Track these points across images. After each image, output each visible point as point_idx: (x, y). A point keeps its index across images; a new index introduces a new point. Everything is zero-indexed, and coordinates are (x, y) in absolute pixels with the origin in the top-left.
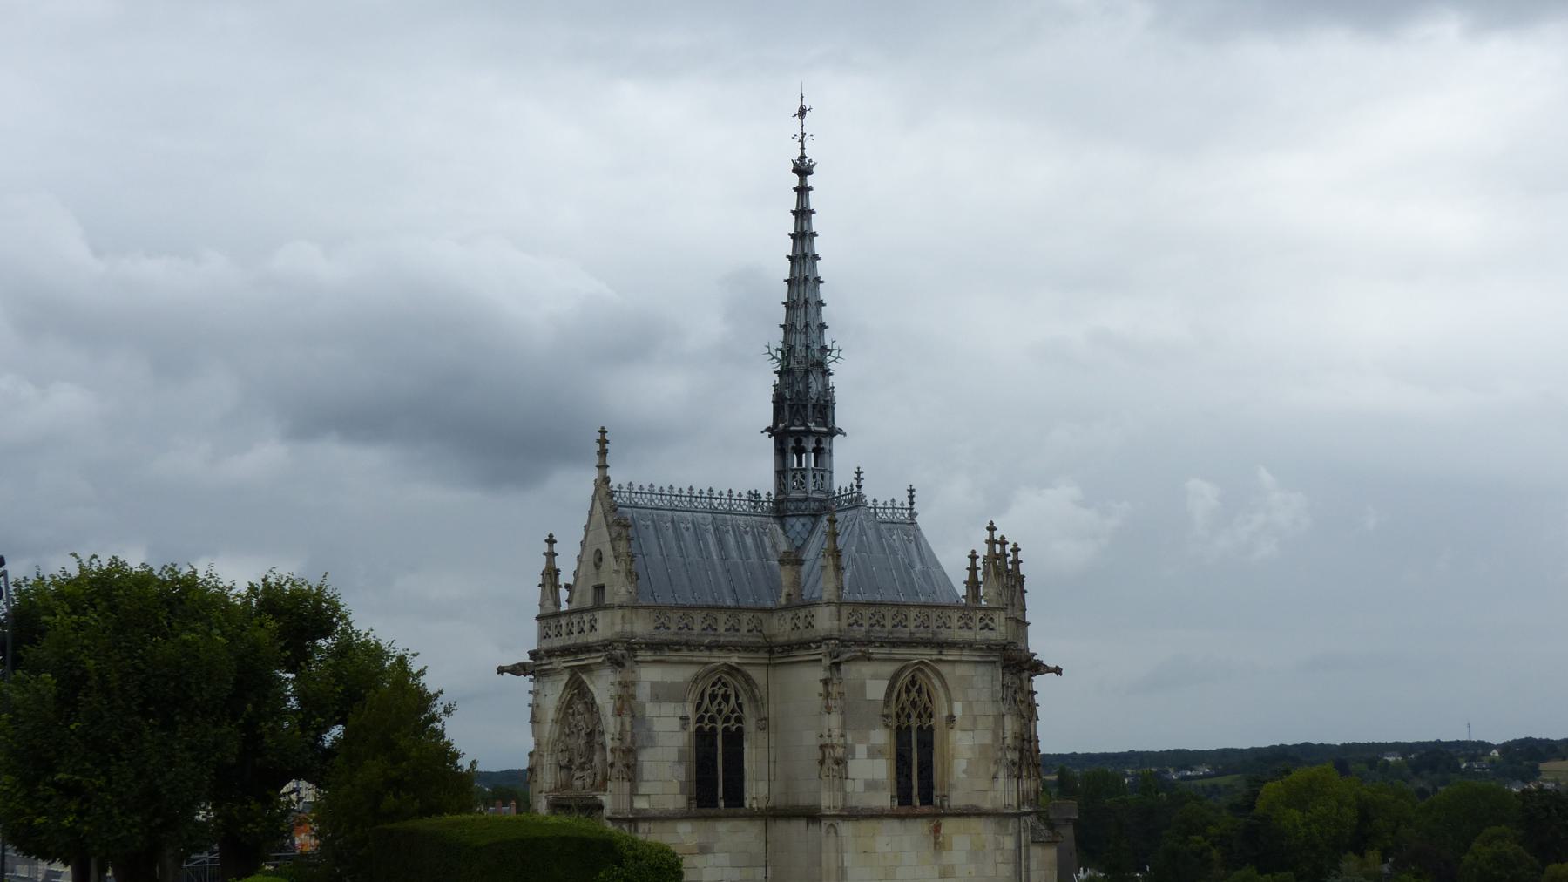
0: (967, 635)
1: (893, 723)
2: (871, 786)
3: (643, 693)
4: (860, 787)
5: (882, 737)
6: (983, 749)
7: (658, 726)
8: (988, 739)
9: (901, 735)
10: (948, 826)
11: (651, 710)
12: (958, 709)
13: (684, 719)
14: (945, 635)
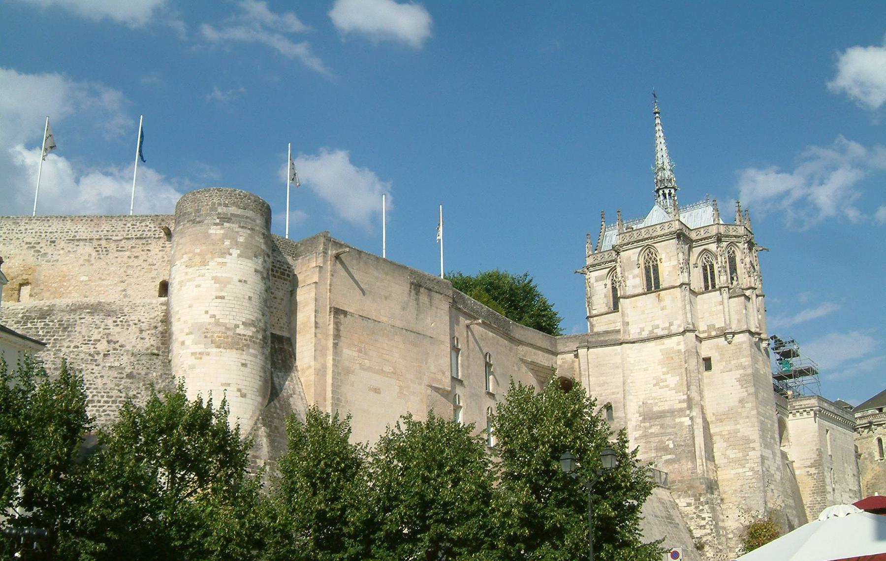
0: (663, 232)
1: (643, 266)
2: (634, 287)
3: (592, 280)
4: (631, 288)
5: (640, 272)
6: (674, 266)
7: (597, 288)
8: (676, 263)
9: (647, 270)
10: (662, 293)
11: (595, 284)
12: (663, 256)
13: (606, 285)
14: (654, 234)
